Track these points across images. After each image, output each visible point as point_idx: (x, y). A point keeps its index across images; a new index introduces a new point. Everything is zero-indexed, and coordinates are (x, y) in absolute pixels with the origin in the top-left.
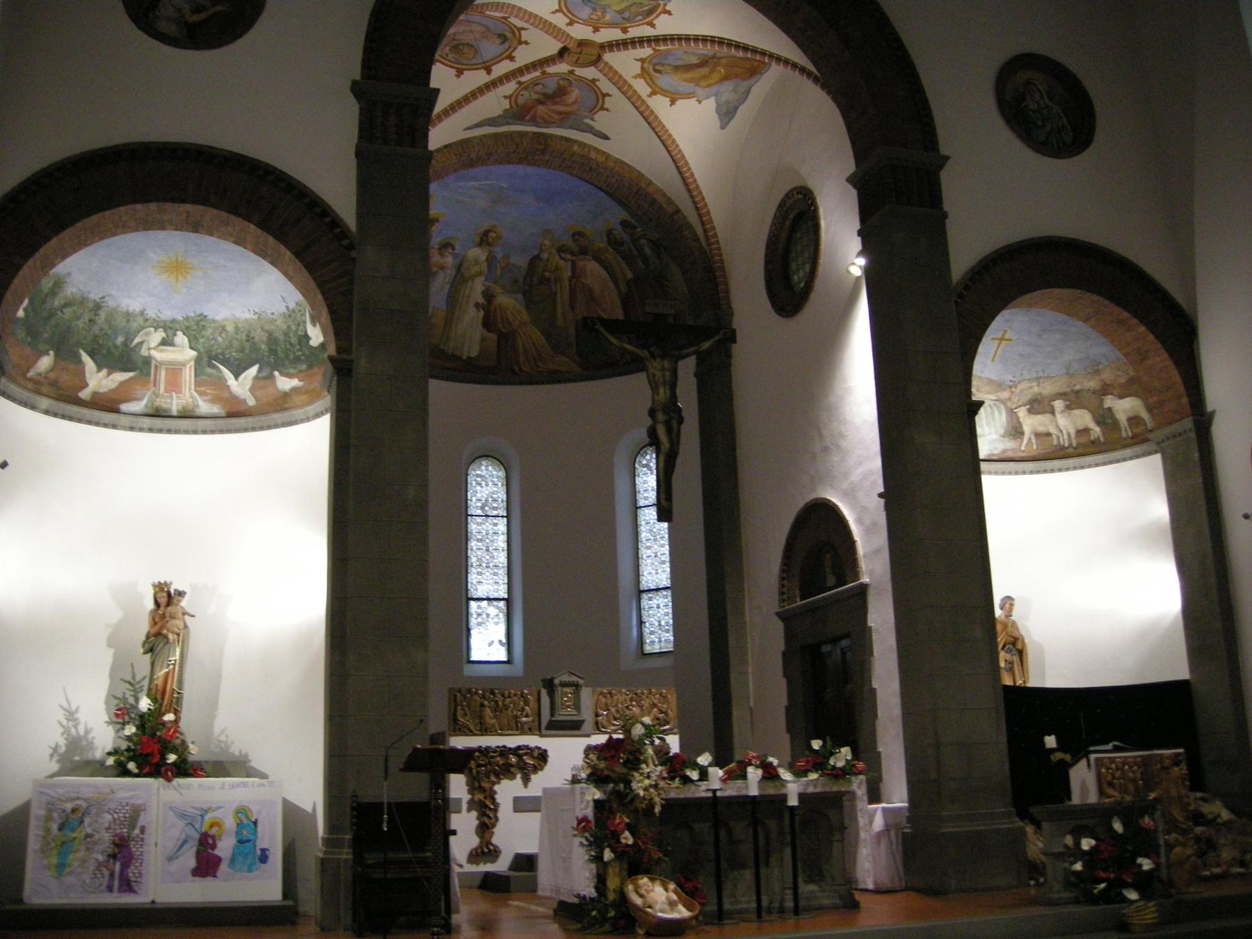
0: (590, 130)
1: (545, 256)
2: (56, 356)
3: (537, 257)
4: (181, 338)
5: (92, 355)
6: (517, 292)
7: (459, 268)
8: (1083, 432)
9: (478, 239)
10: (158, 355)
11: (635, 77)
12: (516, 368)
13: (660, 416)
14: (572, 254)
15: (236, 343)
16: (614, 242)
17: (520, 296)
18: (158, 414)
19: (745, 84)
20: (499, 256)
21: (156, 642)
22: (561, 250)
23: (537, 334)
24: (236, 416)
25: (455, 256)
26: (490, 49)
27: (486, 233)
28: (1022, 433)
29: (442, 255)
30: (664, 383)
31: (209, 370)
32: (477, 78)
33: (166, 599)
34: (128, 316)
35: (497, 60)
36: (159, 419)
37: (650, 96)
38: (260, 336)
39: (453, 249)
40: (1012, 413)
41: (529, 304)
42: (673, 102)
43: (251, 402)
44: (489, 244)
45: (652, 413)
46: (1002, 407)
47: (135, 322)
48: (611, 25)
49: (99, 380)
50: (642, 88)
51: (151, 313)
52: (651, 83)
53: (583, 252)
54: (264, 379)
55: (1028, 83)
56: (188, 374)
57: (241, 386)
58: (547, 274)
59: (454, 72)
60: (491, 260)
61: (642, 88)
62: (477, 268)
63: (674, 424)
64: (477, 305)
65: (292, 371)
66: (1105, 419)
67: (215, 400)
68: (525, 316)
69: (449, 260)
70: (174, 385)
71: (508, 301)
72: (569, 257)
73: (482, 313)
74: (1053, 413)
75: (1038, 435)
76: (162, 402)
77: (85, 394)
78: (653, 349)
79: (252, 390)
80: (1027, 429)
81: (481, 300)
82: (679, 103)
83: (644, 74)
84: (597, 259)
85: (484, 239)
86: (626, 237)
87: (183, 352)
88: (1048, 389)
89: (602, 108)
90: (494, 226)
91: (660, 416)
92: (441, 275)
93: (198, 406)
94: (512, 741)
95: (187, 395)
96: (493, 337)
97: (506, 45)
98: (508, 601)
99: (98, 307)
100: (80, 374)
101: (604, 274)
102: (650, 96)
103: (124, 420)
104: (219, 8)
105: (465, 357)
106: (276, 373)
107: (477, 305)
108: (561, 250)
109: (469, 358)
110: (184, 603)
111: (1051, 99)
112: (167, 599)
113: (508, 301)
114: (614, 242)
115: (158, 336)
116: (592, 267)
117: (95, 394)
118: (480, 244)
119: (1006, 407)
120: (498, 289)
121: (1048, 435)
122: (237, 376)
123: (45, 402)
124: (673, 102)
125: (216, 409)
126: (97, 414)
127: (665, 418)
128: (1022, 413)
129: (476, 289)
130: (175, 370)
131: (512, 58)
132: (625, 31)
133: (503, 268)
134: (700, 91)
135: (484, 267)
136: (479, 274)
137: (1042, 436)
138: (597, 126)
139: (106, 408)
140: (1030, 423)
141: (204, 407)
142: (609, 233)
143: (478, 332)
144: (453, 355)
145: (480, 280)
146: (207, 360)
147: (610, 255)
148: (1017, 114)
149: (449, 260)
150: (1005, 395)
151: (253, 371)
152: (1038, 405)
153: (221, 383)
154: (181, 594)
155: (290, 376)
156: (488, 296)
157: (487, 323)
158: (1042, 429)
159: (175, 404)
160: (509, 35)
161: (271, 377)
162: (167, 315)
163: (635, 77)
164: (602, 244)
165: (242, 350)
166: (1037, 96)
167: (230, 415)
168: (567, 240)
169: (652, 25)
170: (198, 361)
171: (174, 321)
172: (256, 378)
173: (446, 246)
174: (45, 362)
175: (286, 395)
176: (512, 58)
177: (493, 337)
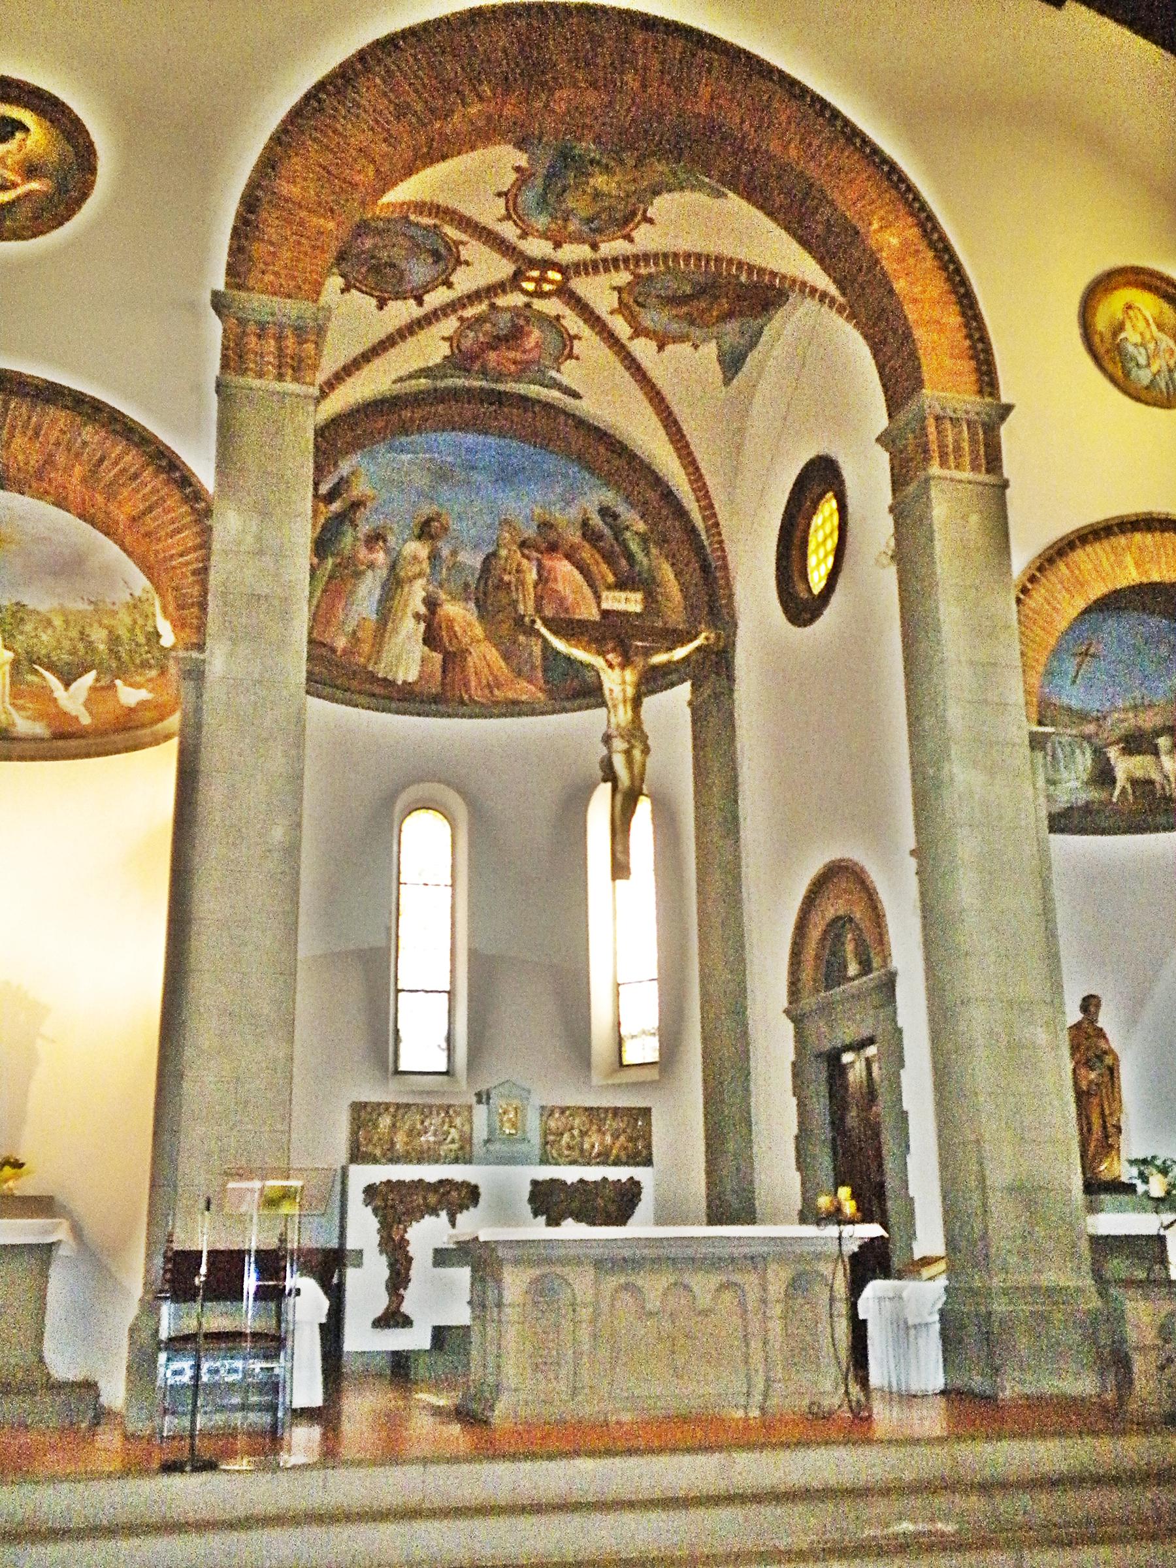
0: (556, 385)
1: (503, 552)
3: (494, 554)
6: (466, 600)
7: (393, 567)
9: (417, 531)
11: (612, 313)
12: (466, 697)
13: (619, 744)
14: (538, 550)
15: (66, 644)
16: (589, 533)
17: (472, 605)
19: (755, 324)
20: (445, 552)
22: (523, 544)
23: (493, 655)
24: (66, 741)
25: (387, 551)
26: (419, 271)
27: (427, 522)
28: (1113, 781)
29: (371, 550)
30: (625, 701)
31: (30, 678)
32: (402, 311)
35: (427, 288)
37: (631, 338)
39: (385, 541)
41: (481, 617)
42: (661, 348)
43: (86, 720)
44: (432, 537)
45: (607, 739)
46: (1085, 744)
48: (578, 239)
50: (621, 327)
52: (632, 320)
53: (553, 548)
58: (506, 578)
59: (374, 302)
60: (434, 557)
61: (621, 327)
62: (416, 569)
63: (637, 753)
64: (417, 616)
65: (138, 679)
67: (38, 717)
68: (479, 631)
69: (380, 557)
71: (459, 613)
72: (535, 554)
73: (423, 626)
75: (1134, 782)
78: (610, 656)
79: (87, 704)
80: (1120, 776)
81: (423, 610)
82: (670, 348)
83: (623, 308)
84: (568, 557)
85: (426, 530)
86: (607, 531)
88: (1149, 721)
89: (570, 356)
90: (439, 515)
91: (619, 744)
92: (370, 573)
93: (14, 725)
94: (431, 1173)
96: (438, 657)
97: (442, 265)
98: (451, 994)
101: (579, 577)
102: (631, 338)
104: (34, 185)
105: (400, 682)
106: (118, 682)
107: (417, 616)
108: (523, 544)
109: (405, 682)
111: (1160, 327)
113: (459, 613)
114: (589, 533)
116: (564, 568)
118: (419, 537)
119: (1091, 744)
120: (443, 596)
121: (1151, 782)
122: (67, 685)
124: (661, 348)
125: (39, 729)
127: (625, 746)
128: (1113, 753)
129: (415, 596)
131: (450, 285)
132: (594, 247)
133: (449, 569)
134: (696, 332)
135: (426, 566)
136: (420, 575)
137: (1142, 785)
138: (565, 380)
140: (1124, 767)
142: (585, 523)
143: (418, 649)
144: (385, 679)
145: (421, 582)
147: (586, 553)
149: (380, 557)
150: (1090, 728)
151: (89, 678)
155: (137, 686)
156: (432, 604)
157: (430, 640)
158: (1139, 774)
160: (443, 251)
161: (112, 687)
163: (612, 313)
164: (574, 536)
165: (73, 652)
166: (1141, 325)
167: (59, 736)
168: (530, 532)
169: (631, 240)
172: (93, 689)
173: (376, 538)
176: (450, 285)
177: (438, 657)
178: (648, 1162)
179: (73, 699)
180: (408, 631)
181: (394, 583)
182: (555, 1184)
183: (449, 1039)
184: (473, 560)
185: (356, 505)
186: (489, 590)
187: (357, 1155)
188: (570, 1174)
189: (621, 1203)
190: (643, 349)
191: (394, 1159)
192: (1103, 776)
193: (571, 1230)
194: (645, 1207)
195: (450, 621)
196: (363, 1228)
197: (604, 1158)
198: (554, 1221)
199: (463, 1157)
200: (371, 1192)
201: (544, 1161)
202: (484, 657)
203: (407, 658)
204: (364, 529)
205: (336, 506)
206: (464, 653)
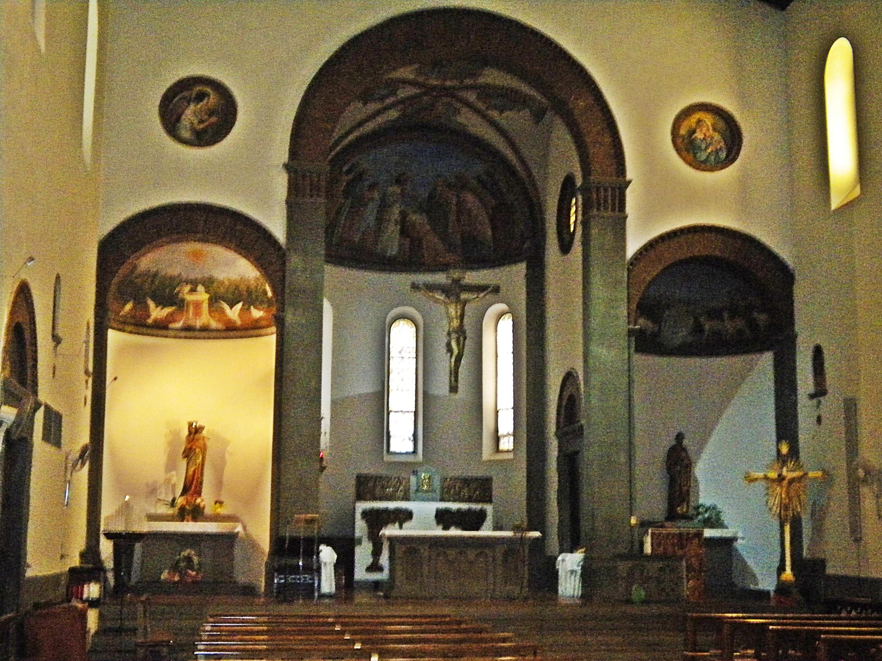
2: (134, 303)
4: (200, 288)
5: (154, 299)
7: (383, 199)
8: (740, 332)
10: (189, 298)
13: (454, 336)
18: (188, 329)
21: (188, 454)
24: (230, 331)
33: (195, 431)
34: (172, 278)
35: (387, 96)
36: (189, 332)
38: (243, 287)
40: (696, 318)
43: (239, 323)
45: (449, 334)
47: (174, 282)
49: (157, 313)
51: (184, 275)
54: (245, 310)
55: (699, 121)
56: (205, 306)
57: (234, 313)
60: (403, 194)
63: (462, 338)
66: (752, 324)
67: (219, 321)
69: (376, 195)
70: (197, 314)
73: (399, 227)
74: (723, 321)
76: (191, 322)
77: (150, 321)
79: (239, 315)
84: (474, 191)
87: (202, 296)
91: (454, 336)
94: (391, 505)
95: (205, 319)
96: (407, 242)
99: (155, 275)
100: (147, 307)
103: (172, 333)
108: (449, 186)
110: (204, 432)
111: (714, 130)
112: (195, 431)
115: (187, 288)
116: (470, 197)
117: (155, 321)
123: (129, 328)
125: (220, 326)
126: (155, 331)
130: (198, 305)
136: (395, 202)
137: (717, 333)
139: (161, 327)
141: (214, 324)
146: (214, 300)
148: (687, 146)
149: (376, 195)
151: (240, 305)
152: (715, 314)
153: (223, 312)
154: (202, 428)
156: (404, 215)
157: (403, 232)
159: (198, 323)
161: (249, 309)
162: (192, 276)
170: (210, 299)
171: (196, 279)
172: (241, 310)
173: (372, 187)
174: (128, 307)
175: (257, 320)
177: (407, 242)
178: (489, 500)
179: (234, 313)
180: (392, 231)
181: (384, 206)
182: (447, 511)
183: (415, 435)
184: (424, 193)
185: (361, 175)
186: (433, 207)
187: (360, 497)
188: (454, 506)
189: (475, 520)
190: (494, 114)
191: (374, 499)
192: (698, 329)
193: (454, 532)
194: (489, 521)
195: (414, 225)
196: (361, 527)
197: (469, 500)
198: (446, 528)
199: (406, 498)
200: (366, 514)
201: (442, 500)
202: (432, 241)
203: (392, 242)
204: (367, 183)
205: (351, 177)
206: (420, 240)
